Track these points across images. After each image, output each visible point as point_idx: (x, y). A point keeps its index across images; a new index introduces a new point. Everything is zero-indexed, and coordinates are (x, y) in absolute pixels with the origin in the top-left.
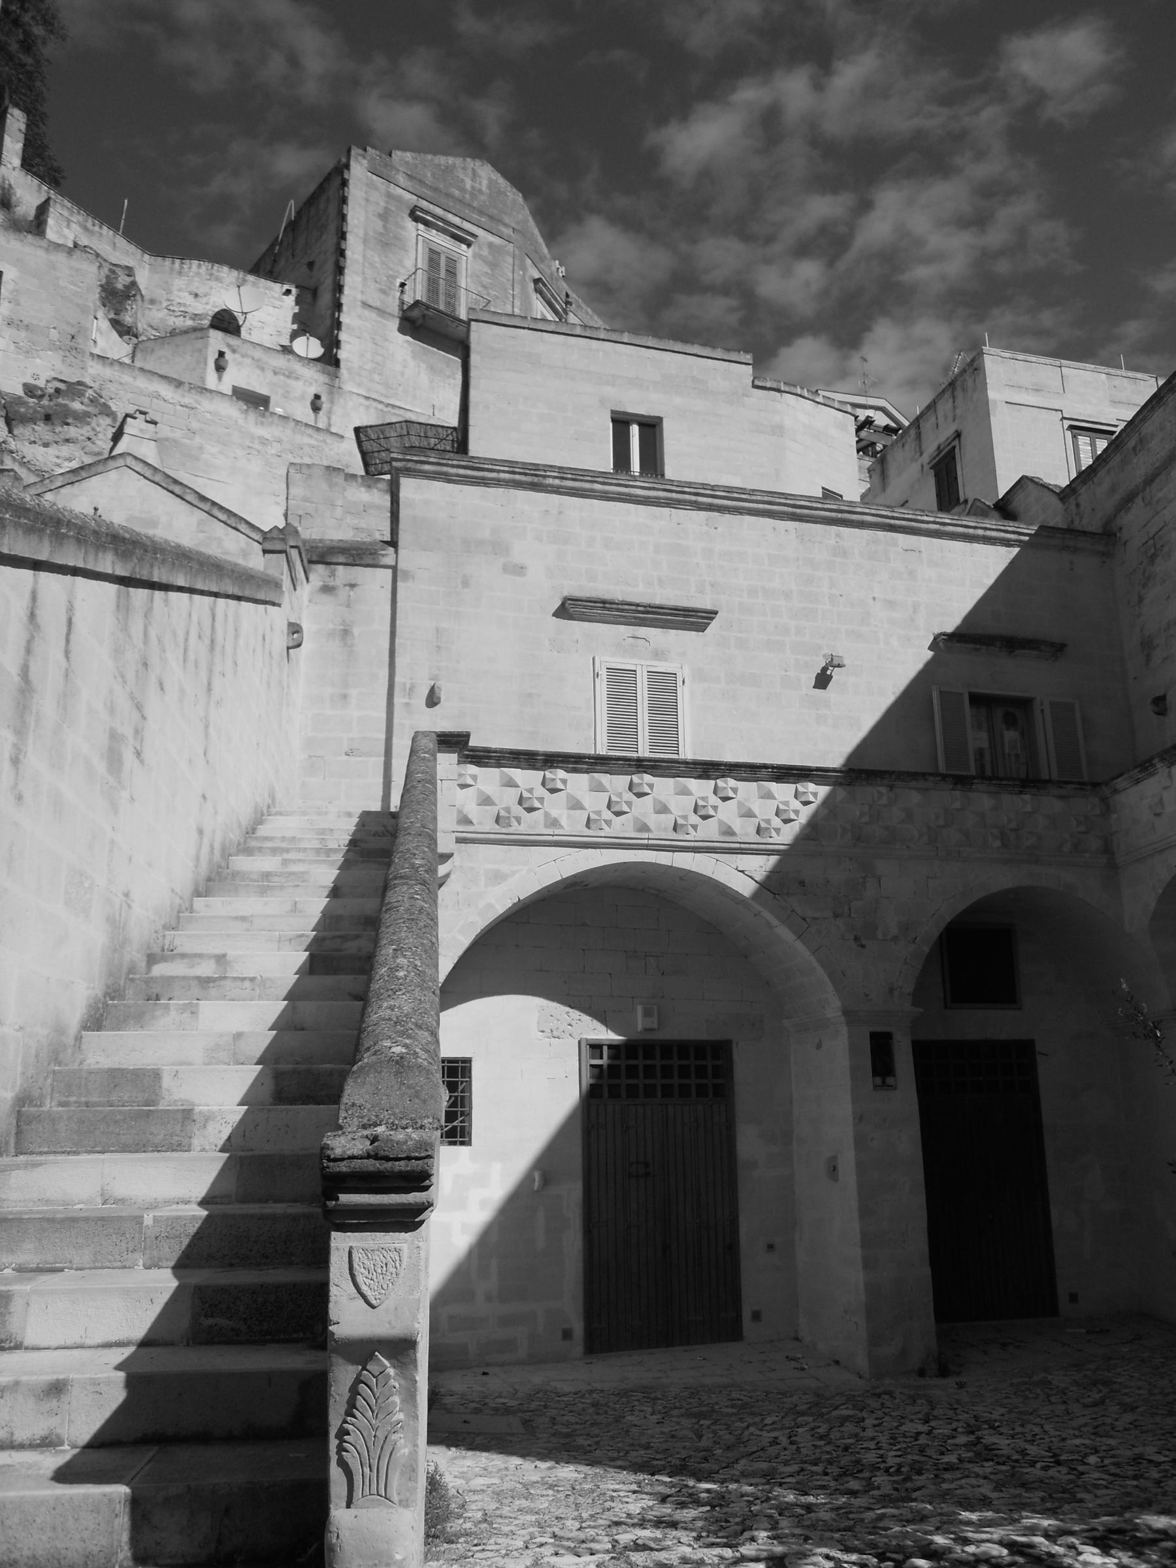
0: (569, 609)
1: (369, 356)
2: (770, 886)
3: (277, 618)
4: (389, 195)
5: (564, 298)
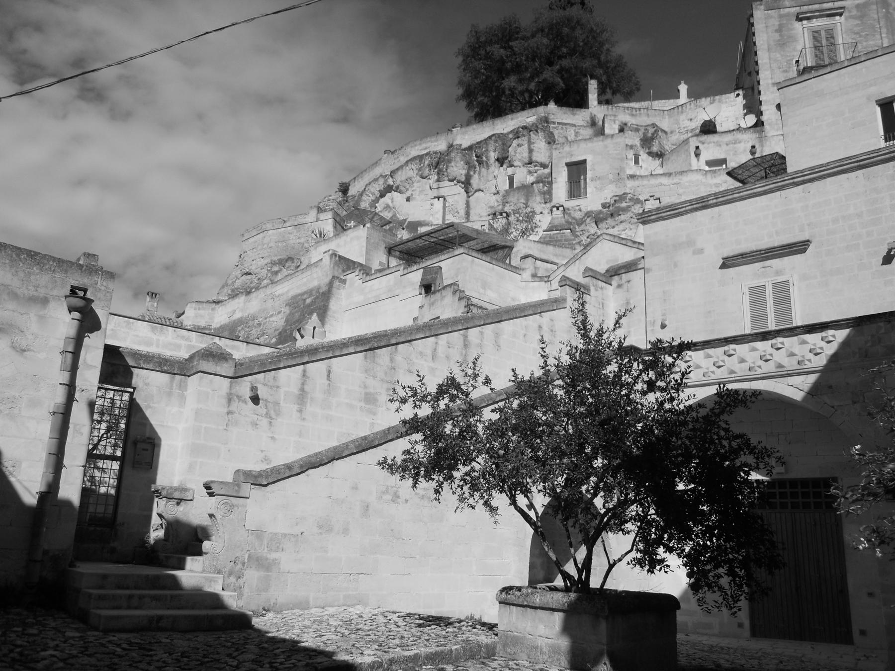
0: (727, 263)
2: (814, 392)
4: (781, 16)
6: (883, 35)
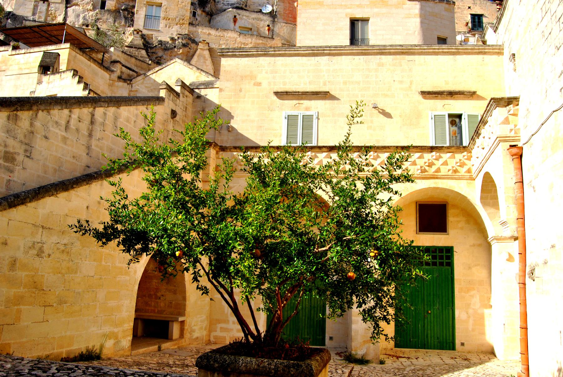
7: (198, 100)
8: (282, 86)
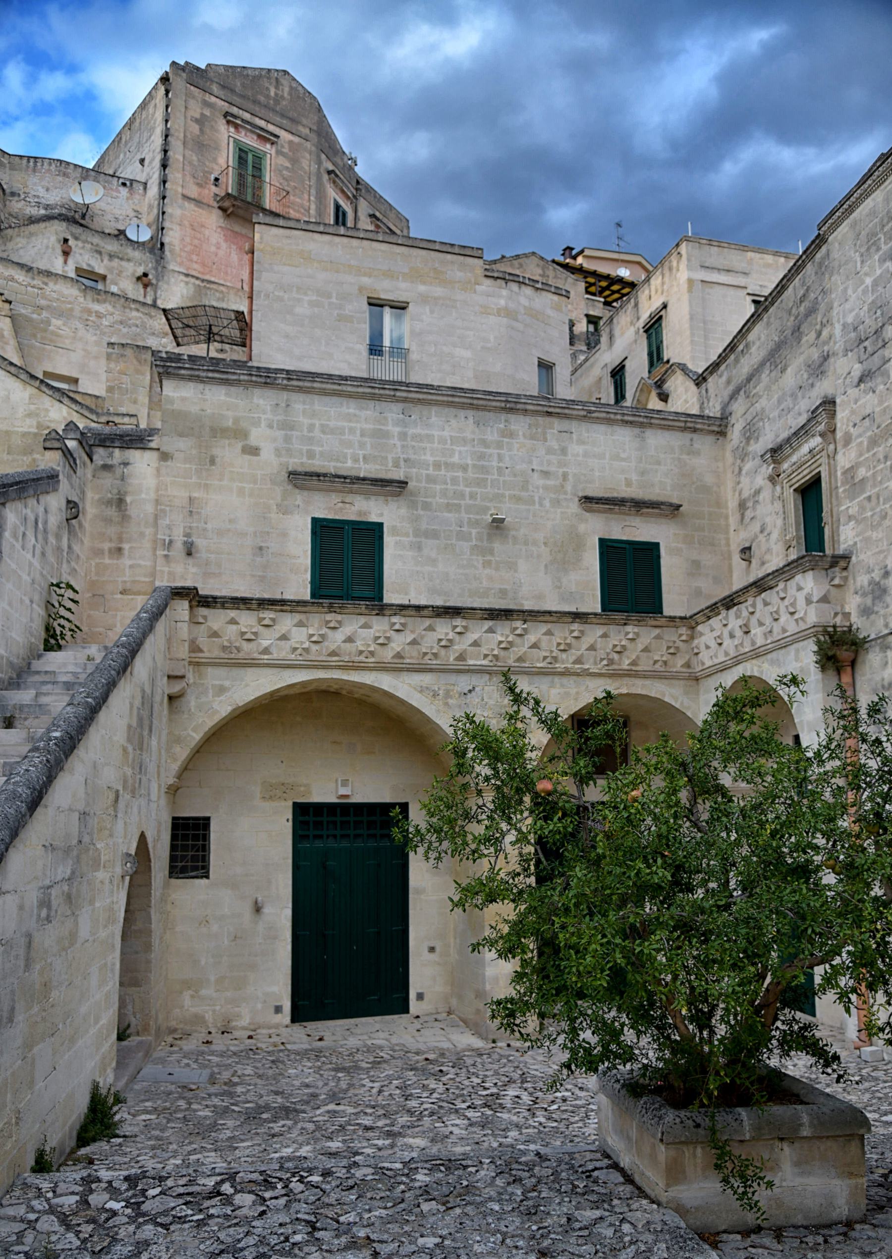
1: (188, 240)
3: (55, 502)
4: (206, 104)
5: (354, 184)
6: (312, 198)
7: (106, 474)
8: (304, 460)
